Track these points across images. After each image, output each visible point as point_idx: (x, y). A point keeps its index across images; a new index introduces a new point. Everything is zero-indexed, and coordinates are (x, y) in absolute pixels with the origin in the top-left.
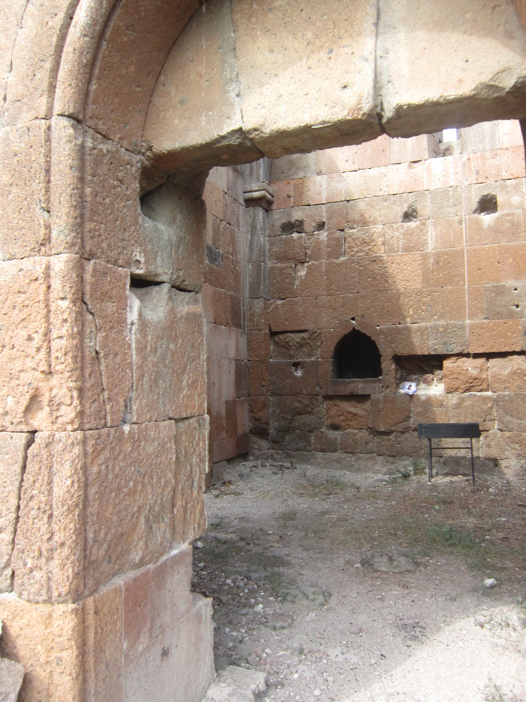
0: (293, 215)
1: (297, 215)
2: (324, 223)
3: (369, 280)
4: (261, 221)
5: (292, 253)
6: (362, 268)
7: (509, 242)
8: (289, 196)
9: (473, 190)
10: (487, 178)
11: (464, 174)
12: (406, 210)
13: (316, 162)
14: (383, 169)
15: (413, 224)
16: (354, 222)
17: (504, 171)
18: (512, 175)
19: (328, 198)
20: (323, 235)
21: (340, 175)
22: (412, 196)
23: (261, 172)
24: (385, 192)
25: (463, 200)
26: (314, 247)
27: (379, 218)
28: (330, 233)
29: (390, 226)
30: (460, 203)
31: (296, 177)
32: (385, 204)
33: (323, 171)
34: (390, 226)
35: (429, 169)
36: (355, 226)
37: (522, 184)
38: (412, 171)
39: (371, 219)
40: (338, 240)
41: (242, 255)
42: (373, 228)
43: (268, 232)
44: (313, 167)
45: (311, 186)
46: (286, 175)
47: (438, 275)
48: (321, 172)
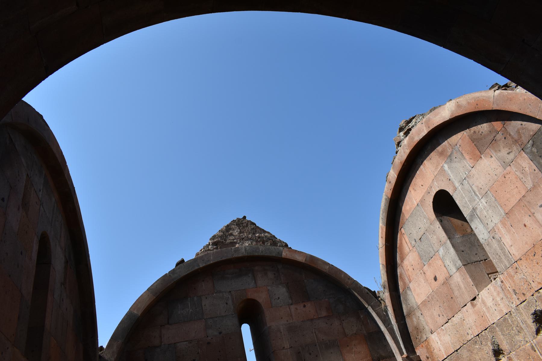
9: (522, 311)
10: (524, 294)
11: (507, 297)
12: (491, 348)
17: (532, 283)
25: (521, 324)
30: (521, 328)
32: (477, 347)
35: (484, 302)
38: (475, 309)
44: (426, 327)
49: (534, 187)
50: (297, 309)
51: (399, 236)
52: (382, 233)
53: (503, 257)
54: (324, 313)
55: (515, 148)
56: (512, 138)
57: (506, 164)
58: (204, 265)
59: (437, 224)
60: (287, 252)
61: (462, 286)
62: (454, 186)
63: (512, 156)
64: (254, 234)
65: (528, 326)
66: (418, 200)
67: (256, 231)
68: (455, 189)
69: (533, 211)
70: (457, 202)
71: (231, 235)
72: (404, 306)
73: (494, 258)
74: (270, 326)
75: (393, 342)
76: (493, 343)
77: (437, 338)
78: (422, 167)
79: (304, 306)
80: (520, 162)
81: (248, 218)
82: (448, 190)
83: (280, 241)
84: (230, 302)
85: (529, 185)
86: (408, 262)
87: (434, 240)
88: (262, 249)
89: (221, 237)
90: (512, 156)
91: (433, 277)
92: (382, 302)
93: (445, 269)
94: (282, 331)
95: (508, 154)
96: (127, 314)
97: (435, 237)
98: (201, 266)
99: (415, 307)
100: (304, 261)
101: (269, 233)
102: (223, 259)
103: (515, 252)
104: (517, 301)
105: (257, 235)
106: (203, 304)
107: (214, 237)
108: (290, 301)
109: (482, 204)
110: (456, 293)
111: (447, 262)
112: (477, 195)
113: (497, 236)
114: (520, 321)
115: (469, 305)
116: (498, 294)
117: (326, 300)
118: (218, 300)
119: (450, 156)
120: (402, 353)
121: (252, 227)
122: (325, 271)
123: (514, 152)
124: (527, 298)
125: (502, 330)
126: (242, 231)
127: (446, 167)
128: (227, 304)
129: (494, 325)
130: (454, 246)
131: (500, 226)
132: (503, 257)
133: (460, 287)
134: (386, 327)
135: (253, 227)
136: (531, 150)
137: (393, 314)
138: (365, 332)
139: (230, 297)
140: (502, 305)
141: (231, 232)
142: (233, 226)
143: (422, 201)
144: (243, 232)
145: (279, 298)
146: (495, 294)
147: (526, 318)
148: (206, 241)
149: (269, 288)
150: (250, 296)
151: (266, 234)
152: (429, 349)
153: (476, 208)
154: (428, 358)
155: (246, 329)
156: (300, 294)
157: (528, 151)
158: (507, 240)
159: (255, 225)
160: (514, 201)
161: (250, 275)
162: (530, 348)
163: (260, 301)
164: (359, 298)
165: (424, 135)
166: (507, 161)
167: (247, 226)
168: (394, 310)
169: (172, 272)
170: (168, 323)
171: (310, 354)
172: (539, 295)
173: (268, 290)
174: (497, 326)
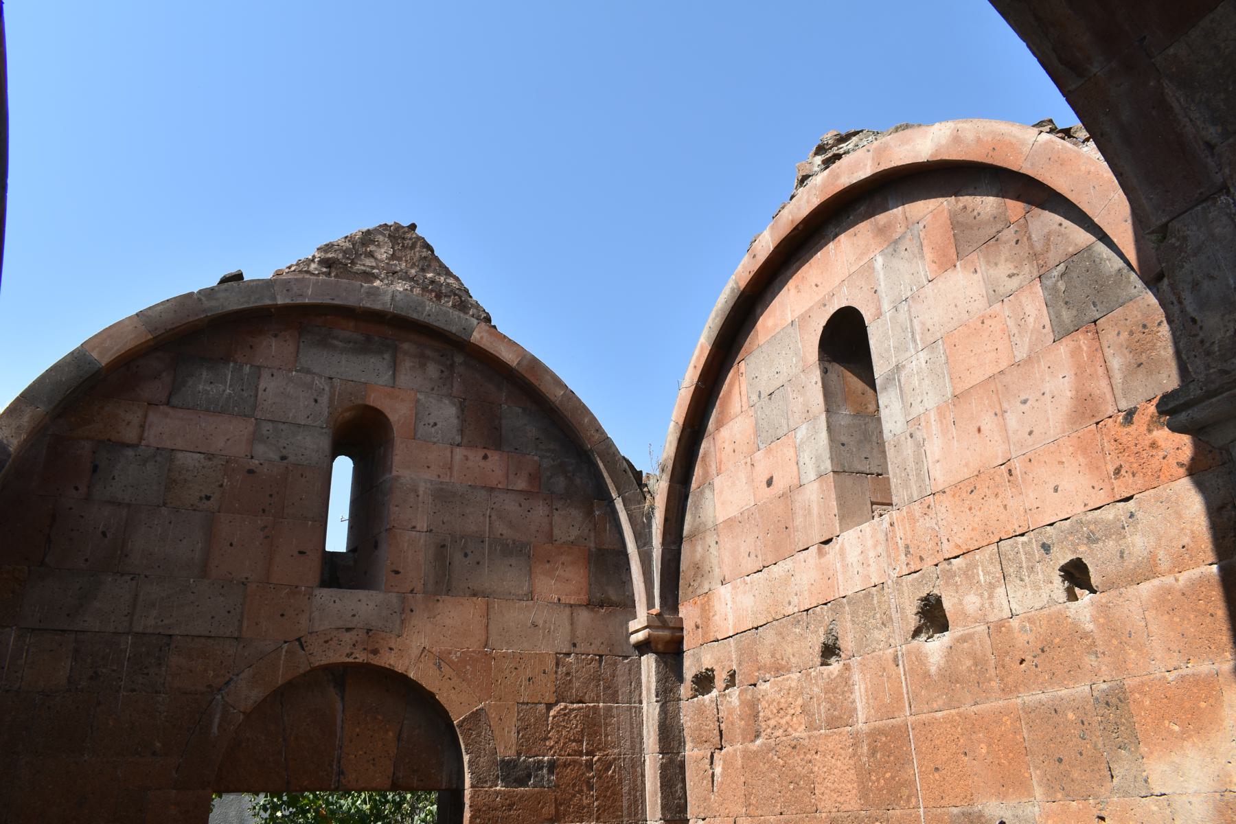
1: (707, 661)
3: (791, 787)
6: (781, 762)
7: (976, 704)
9: (905, 589)
10: (921, 559)
11: (889, 556)
12: (822, 639)
15: (835, 666)
17: (945, 541)
18: (958, 546)
19: (734, 626)
27: (793, 660)
30: (891, 618)
35: (842, 552)
37: (976, 566)
38: (822, 560)
39: (784, 663)
44: (717, 570)
47: (878, 780)
49: (1029, 360)
50: (467, 458)
51: (730, 375)
52: (698, 359)
53: (913, 479)
54: (521, 484)
55: (1027, 268)
56: (1032, 246)
57: (996, 296)
58: (288, 301)
59: (816, 375)
60: (485, 335)
61: (815, 510)
62: (879, 308)
63: (1014, 284)
64: (423, 270)
65: (904, 618)
66: (797, 314)
67: (429, 266)
68: (879, 315)
69: (1005, 406)
70: (872, 342)
71: (371, 255)
72: (688, 518)
74: (398, 477)
75: (641, 579)
76: (829, 632)
77: (728, 596)
78: (831, 245)
79: (485, 457)
80: (1024, 300)
81: (419, 232)
82: (863, 312)
83: (477, 306)
84: (324, 400)
85: (1021, 354)
86: (729, 434)
87: (797, 404)
88: (431, 311)
89: (345, 252)
90: (1014, 284)
92: (648, 496)
93: (795, 468)
94: (421, 493)
95: (1010, 276)
96: (72, 353)
97: (801, 399)
98: (280, 302)
99: (710, 525)
100: (514, 364)
101: (457, 279)
102: (336, 302)
103: (940, 476)
104: (904, 567)
105: (430, 275)
106: (262, 386)
107: (328, 247)
108: (458, 439)
109: (917, 362)
110: (799, 521)
111: (806, 457)
112: (915, 341)
113: (918, 435)
114: (893, 606)
115: (813, 550)
116: (875, 546)
117: (536, 458)
118: (296, 388)
119: (896, 242)
120: (650, 605)
121: (424, 254)
122: (552, 398)
123: (1021, 277)
124: (924, 568)
125: (854, 613)
126: (398, 254)
128: (316, 401)
130: (830, 428)
131: (933, 416)
132: (913, 479)
133: (810, 512)
134: (638, 548)
135: (425, 253)
136: (1055, 284)
137: (661, 527)
138: (592, 545)
139: (327, 388)
140: (873, 568)
141: (372, 248)
142: (381, 238)
143: (805, 318)
144: (399, 259)
145: (435, 424)
146: (870, 543)
147: (907, 602)
148: (307, 249)
149: (420, 396)
150: (374, 400)
151: (451, 281)
152: (706, 611)
153: (904, 366)
154: (697, 627)
155: (343, 468)
156: (484, 429)
157: (1049, 283)
158: (934, 448)
159: (432, 251)
160: (979, 376)
161: (387, 356)
162: (891, 658)
163: (393, 417)
164: (606, 475)
165: (863, 177)
166: (1001, 290)
167: (413, 247)
168: (666, 520)
169: (209, 293)
170: (168, 403)
171: (466, 555)
172: (948, 567)
173: (418, 401)
174: (849, 603)
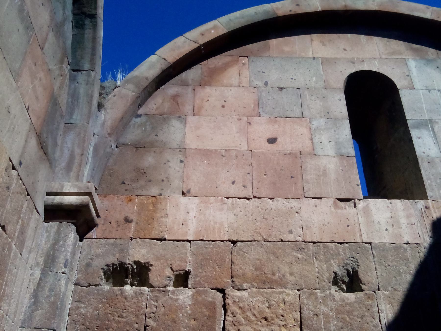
0: (131, 252)
1: (138, 253)
2: (187, 274)
4: (70, 249)
5: (118, 322)
8: (127, 221)
13: (182, 177)
14: (294, 203)
16: (244, 277)
20: (185, 295)
21: (222, 200)
22: (344, 249)
23: (87, 171)
24: (296, 236)
26: (164, 314)
27: (291, 278)
28: (197, 292)
29: (311, 294)
31: (144, 192)
32: (299, 256)
33: (192, 191)
34: (311, 294)
35: (367, 211)
36: (245, 285)
38: (339, 211)
39: (276, 277)
40: (212, 307)
41: (13, 307)
42: (280, 293)
43: (75, 276)
44: (176, 183)
45: (170, 209)
46: (128, 187)
48: (189, 191)
61: (333, 176)
66: (319, 55)
73: (429, 179)
78: (363, 38)
87: (314, 105)
91: (270, 136)
93: (308, 143)
99: (175, 145)
110: (310, 176)
116: (408, 216)
127: (412, 64)
129: (369, 246)
153: (437, 123)
